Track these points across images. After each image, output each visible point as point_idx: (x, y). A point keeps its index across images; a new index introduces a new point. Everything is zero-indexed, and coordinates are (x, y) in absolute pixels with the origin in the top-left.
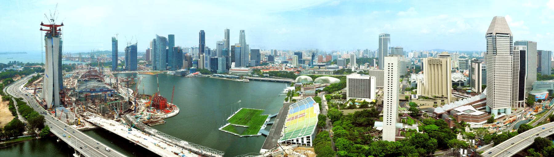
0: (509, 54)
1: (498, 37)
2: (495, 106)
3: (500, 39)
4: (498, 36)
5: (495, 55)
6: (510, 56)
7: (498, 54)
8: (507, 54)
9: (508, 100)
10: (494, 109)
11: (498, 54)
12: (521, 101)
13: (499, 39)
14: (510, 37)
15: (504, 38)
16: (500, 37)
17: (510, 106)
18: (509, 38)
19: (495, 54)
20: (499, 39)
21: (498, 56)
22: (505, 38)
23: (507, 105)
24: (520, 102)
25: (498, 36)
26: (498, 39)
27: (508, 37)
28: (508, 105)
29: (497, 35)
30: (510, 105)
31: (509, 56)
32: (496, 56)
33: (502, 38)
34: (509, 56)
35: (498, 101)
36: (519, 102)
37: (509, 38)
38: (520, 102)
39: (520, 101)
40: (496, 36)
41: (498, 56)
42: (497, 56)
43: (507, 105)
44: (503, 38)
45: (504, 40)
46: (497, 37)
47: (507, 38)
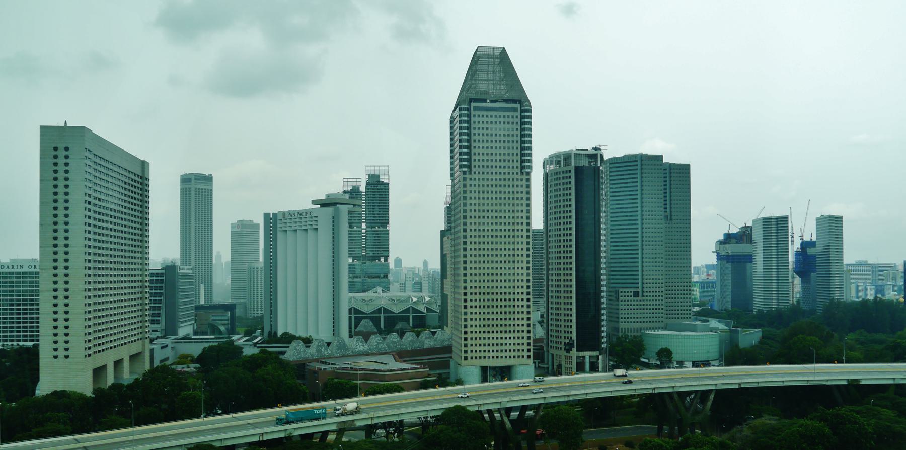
0: (516, 170)
1: (477, 113)
2: (469, 355)
3: (485, 119)
4: (476, 109)
5: (464, 172)
6: (520, 177)
7: (477, 170)
8: (511, 170)
9: (521, 335)
10: (463, 363)
11: (477, 170)
12: (587, 354)
14: (522, 111)
16: (485, 113)
17: (529, 357)
18: (515, 114)
19: (464, 166)
20: (481, 119)
21: (476, 176)
22: (502, 114)
23: (516, 354)
24: (584, 357)
25: (476, 109)
26: (476, 119)
27: (515, 110)
28: (521, 354)
29: (473, 104)
31: (516, 177)
32: (468, 176)
33: (490, 113)
34: (516, 177)
35: (478, 336)
36: (578, 357)
37: (518, 114)
38: (584, 357)
39: (582, 354)
40: (469, 109)
41: (476, 176)
42: (473, 176)
43: (516, 354)
44: (494, 113)
46: (473, 113)
47: (511, 114)
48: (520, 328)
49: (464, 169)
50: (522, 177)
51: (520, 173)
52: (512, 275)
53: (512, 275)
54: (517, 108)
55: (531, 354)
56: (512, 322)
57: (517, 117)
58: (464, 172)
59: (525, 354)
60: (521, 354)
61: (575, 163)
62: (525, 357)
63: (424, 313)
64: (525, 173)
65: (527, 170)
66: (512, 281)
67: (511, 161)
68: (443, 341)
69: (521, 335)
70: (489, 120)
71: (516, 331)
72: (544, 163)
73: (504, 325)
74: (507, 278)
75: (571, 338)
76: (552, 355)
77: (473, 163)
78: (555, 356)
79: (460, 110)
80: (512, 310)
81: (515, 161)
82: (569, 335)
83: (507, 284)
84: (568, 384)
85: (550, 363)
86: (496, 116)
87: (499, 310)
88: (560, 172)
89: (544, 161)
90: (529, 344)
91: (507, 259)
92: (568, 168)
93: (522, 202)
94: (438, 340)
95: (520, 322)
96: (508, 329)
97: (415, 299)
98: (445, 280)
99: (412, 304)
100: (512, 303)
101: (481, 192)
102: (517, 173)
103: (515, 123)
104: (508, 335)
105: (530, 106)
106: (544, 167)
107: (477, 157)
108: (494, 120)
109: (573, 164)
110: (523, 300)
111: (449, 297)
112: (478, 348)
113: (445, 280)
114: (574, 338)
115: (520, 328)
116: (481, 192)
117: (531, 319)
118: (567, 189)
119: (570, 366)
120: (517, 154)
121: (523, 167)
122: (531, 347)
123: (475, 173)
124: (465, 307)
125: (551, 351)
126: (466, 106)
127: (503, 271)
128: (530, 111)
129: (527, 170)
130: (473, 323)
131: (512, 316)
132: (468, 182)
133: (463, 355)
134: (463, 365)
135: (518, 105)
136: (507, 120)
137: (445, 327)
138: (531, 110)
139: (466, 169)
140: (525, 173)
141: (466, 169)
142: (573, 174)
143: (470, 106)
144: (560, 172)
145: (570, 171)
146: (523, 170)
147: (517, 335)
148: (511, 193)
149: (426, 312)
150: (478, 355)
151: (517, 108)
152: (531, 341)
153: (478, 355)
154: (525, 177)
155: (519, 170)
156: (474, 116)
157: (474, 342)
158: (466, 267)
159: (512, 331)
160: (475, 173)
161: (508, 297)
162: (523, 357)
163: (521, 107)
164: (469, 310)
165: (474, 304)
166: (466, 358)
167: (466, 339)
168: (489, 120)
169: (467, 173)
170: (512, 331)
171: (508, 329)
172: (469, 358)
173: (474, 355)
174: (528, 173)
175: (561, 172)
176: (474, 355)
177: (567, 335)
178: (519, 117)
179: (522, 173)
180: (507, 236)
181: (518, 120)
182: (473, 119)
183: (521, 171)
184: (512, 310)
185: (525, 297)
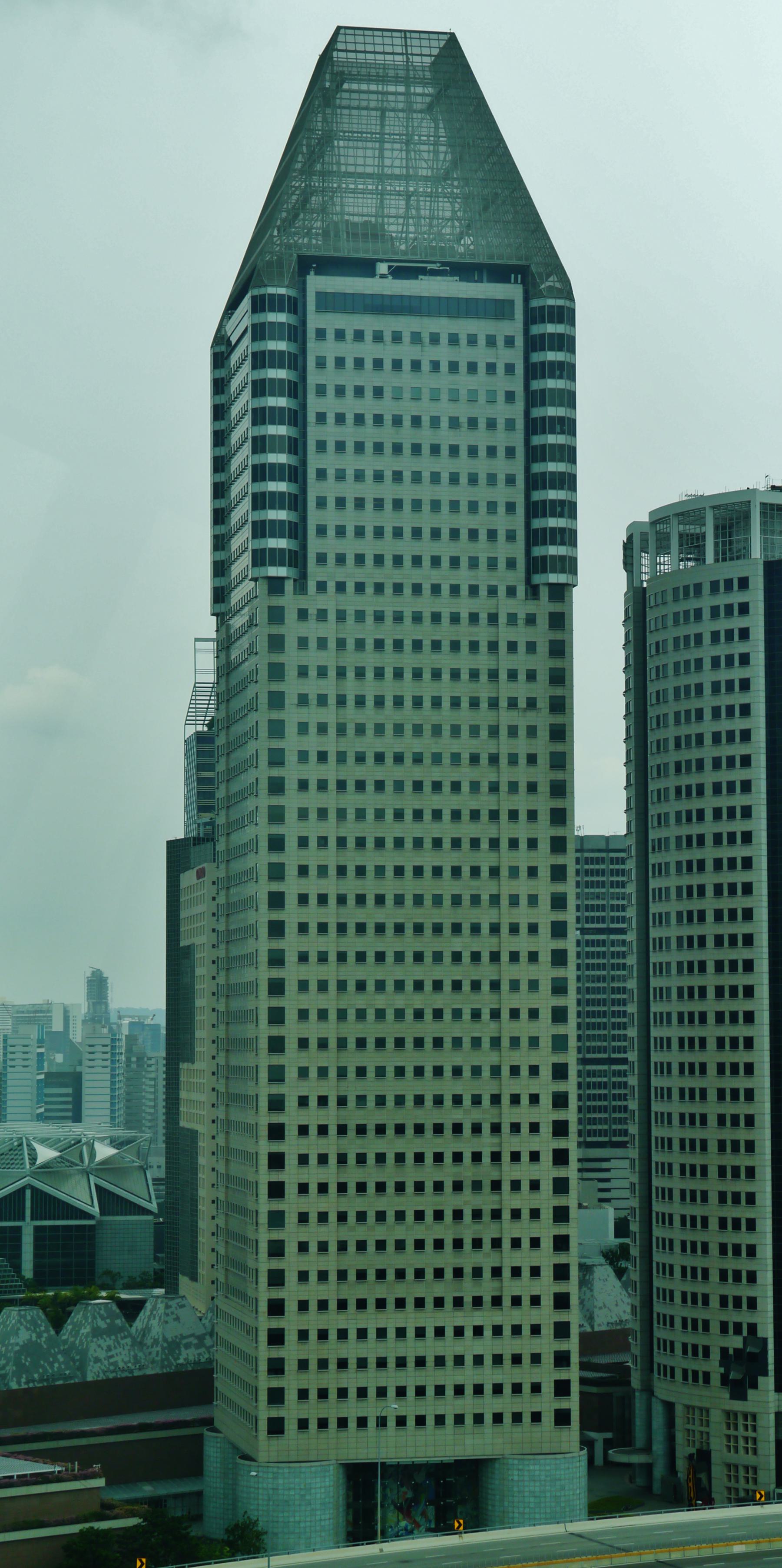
1: (332, 321)
2: (291, 1410)
3: (368, 350)
4: (327, 302)
5: (276, 585)
6: (520, 606)
7: (330, 573)
9: (525, 1316)
11: (330, 573)
13: (349, 350)
14: (532, 317)
15: (428, 325)
16: (369, 323)
17: (562, 1418)
20: (349, 350)
21: (330, 602)
22: (443, 326)
23: (506, 1404)
25: (327, 302)
26: (330, 349)
28: (526, 1404)
29: (316, 283)
30: (547, 1403)
32: (289, 600)
33: (388, 324)
35: (333, 1320)
37: (515, 327)
40: (295, 306)
41: (330, 602)
42: (313, 602)
43: (506, 1404)
44: (406, 324)
45: (427, 354)
46: (314, 320)
47: (482, 327)
48: (525, 1287)
49: (274, 571)
50: (531, 607)
51: (521, 590)
52: (486, 1043)
53: (486, 1043)
54: (512, 302)
55: (573, 1403)
56: (486, 1259)
57: (510, 342)
58: (276, 585)
59: (547, 1403)
60: (526, 1404)
61: (765, 549)
62: (548, 1418)
63: (90, 1217)
64: (544, 592)
65: (553, 578)
66: (486, 1073)
67: (483, 535)
68: (173, 1346)
69: (525, 1316)
70: (388, 352)
71: (507, 1302)
72: (628, 547)
73: (449, 1274)
74: (465, 1058)
75: (753, 1328)
76: (669, 1407)
77: (314, 545)
78: (679, 1411)
79: (258, 305)
80: (486, 1201)
81: (501, 536)
82: (745, 1317)
83: (465, 1087)
84: (738, 1549)
85: (659, 1447)
86: (416, 338)
87: (428, 1202)
88: (698, 588)
89: (630, 538)
90: (562, 1360)
91: (465, 972)
92: (733, 570)
93: (531, 718)
94: (149, 1341)
95: (525, 1258)
96: (468, 1289)
97: (45, 1154)
98: (184, 1066)
99: (33, 1175)
100: (486, 1171)
101: (351, 674)
102: (511, 591)
103: (500, 369)
104: (469, 1318)
105: (568, 294)
106: (629, 563)
107: (331, 517)
108: (407, 352)
109: (756, 552)
110: (535, 1156)
111: (204, 1144)
112: (332, 1380)
113: (184, 1066)
114: (767, 1330)
115: (525, 1287)
116: (351, 674)
117: (573, 1243)
118: (730, 660)
119: (750, 1459)
120: (511, 507)
121: (536, 565)
122: (573, 1374)
123: (322, 587)
124: (276, 1190)
125: (663, 1389)
126: (282, 291)
127: (448, 1029)
128: (566, 315)
129: (553, 578)
130: (313, 1262)
131: (488, 1231)
132: (292, 629)
133: (265, 1412)
134: (262, 1457)
135: (512, 291)
136: (464, 354)
137: (184, 1281)
138: (572, 311)
139: (281, 572)
140: (544, 592)
141: (281, 572)
142: (756, 597)
143: (303, 290)
144: (698, 588)
145: (744, 583)
146: (537, 579)
147: (507, 1317)
148: (484, 677)
149: (96, 1210)
150: (332, 1410)
151: (512, 302)
152: (573, 1345)
153: (332, 1410)
154: (544, 607)
155: (517, 578)
156: (321, 334)
157: (313, 1350)
158: (281, 1361)
159: (487, 1300)
160: (322, 587)
161: (467, 1145)
162: (536, 1417)
163: (526, 300)
164: (291, 1204)
165: (314, 1175)
166: (276, 1427)
167: (276, 1338)
168: (388, 352)
169: (289, 586)
170: (487, 1300)
171: (468, 1289)
172: (291, 1426)
173: (313, 1410)
174: (561, 593)
175: (706, 588)
176: (313, 1410)
177: (732, 1316)
178: (519, 341)
179: (533, 591)
180: (466, 871)
181: (516, 356)
182: (314, 348)
183: (528, 581)
184: (486, 1201)
185: (546, 1143)
